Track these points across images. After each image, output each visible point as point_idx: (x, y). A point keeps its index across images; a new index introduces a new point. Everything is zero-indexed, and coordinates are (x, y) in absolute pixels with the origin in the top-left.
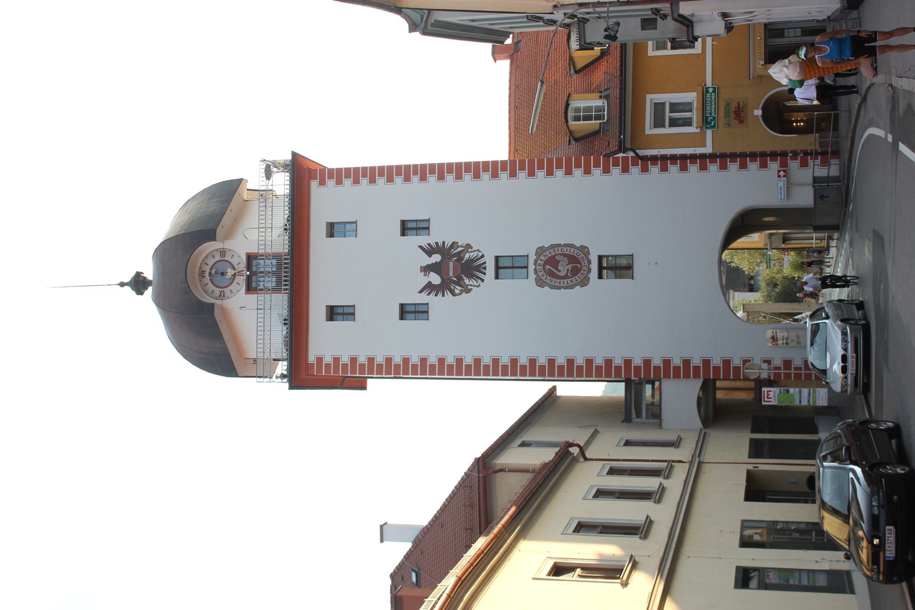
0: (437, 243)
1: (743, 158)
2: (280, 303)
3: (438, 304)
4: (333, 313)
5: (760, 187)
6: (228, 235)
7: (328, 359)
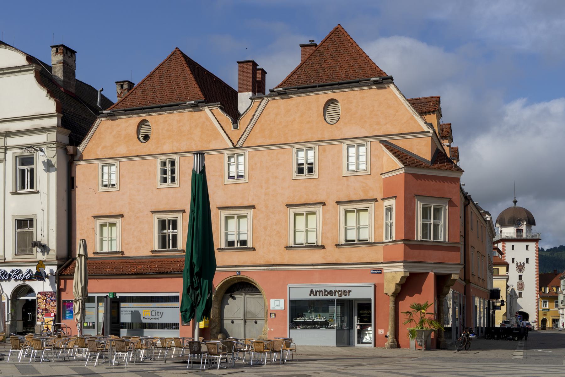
1: (538, 315)
2: (514, 236)
3: (515, 265)
4: (513, 246)
5: (532, 318)
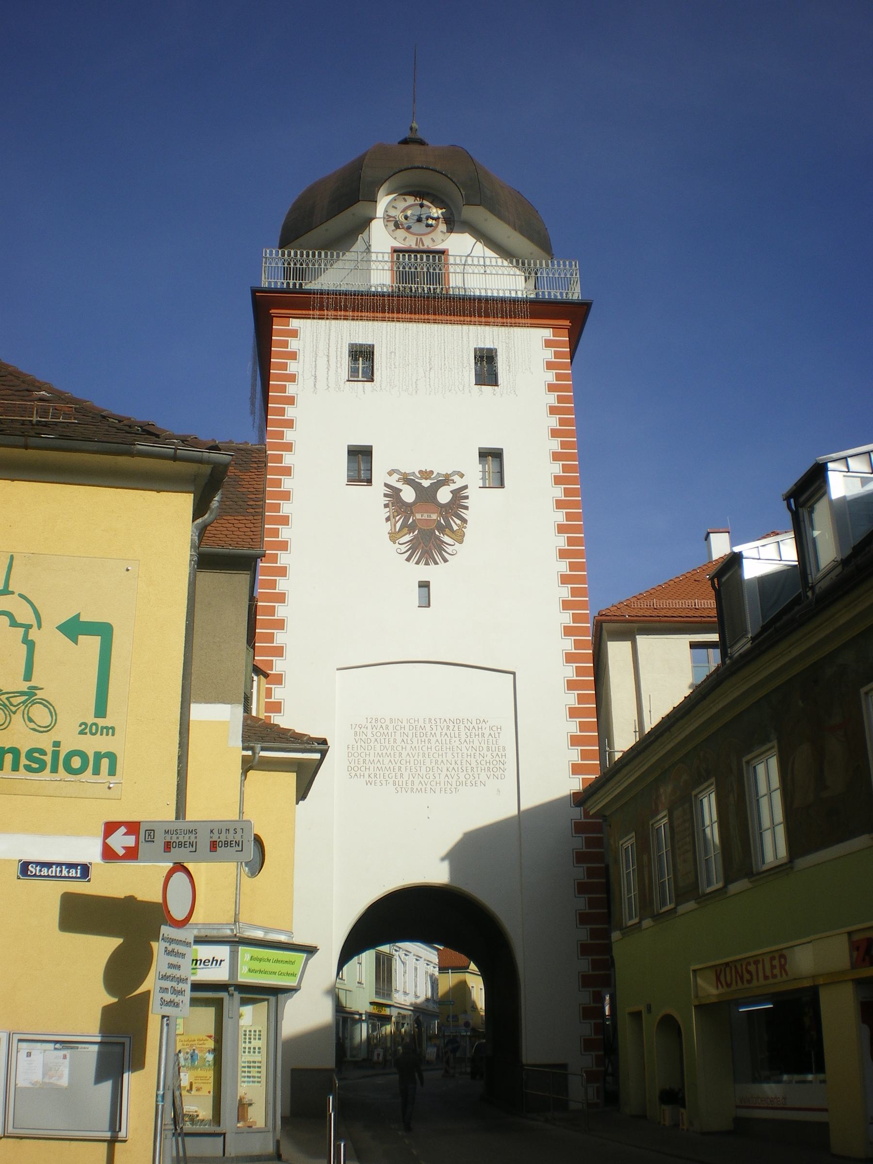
0: (467, 497)
3: (372, 497)
7: (294, 344)
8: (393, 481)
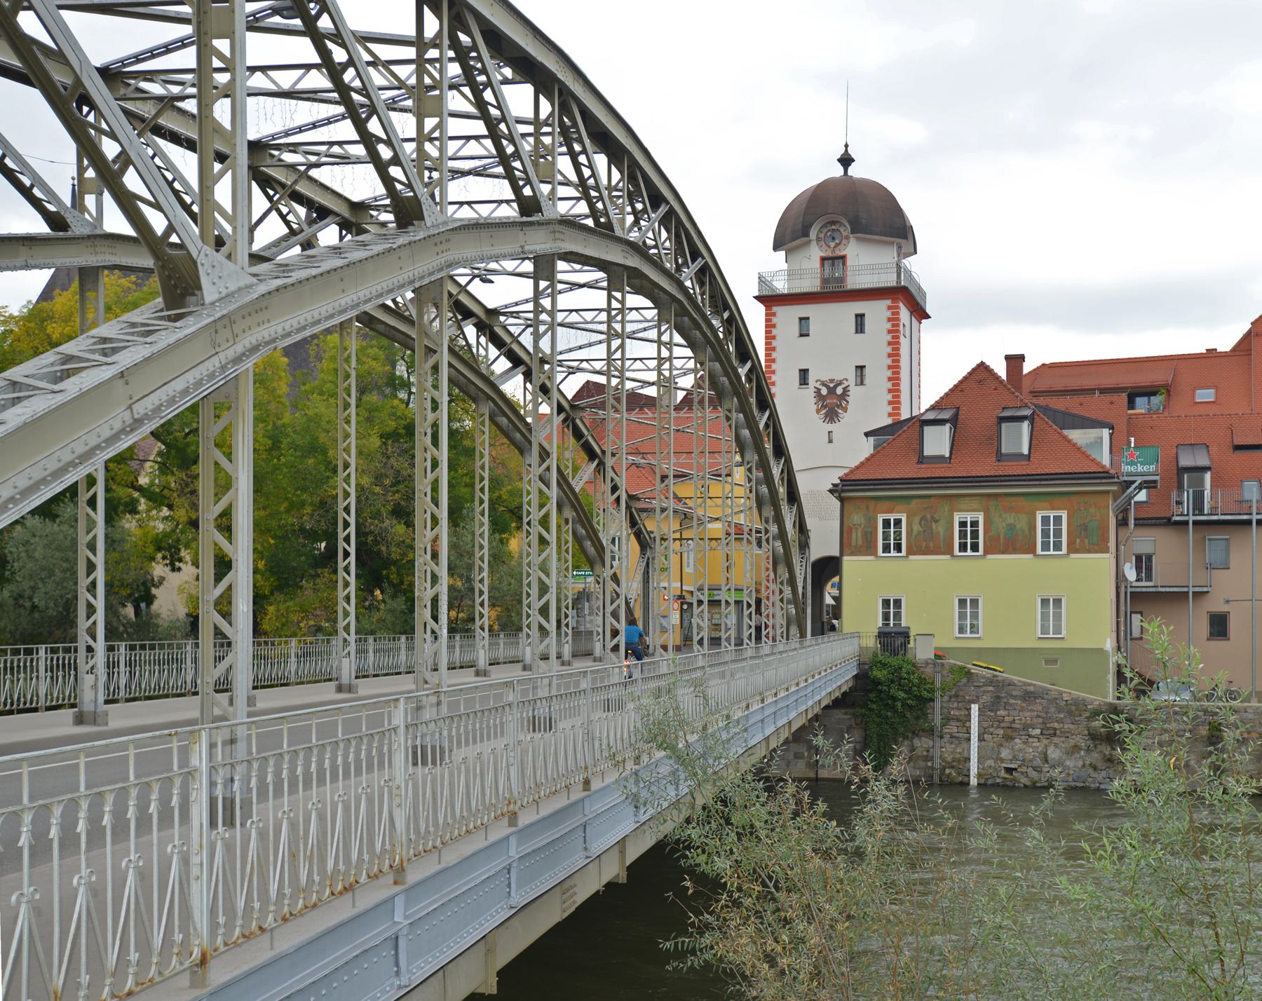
3: (809, 392)
4: (804, 320)
6: (858, 239)
8: (818, 385)
